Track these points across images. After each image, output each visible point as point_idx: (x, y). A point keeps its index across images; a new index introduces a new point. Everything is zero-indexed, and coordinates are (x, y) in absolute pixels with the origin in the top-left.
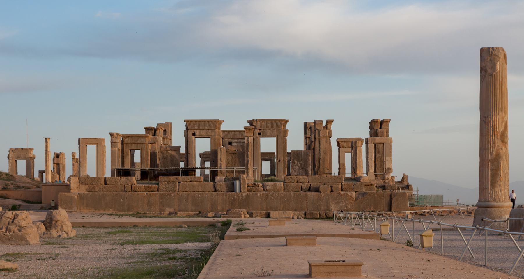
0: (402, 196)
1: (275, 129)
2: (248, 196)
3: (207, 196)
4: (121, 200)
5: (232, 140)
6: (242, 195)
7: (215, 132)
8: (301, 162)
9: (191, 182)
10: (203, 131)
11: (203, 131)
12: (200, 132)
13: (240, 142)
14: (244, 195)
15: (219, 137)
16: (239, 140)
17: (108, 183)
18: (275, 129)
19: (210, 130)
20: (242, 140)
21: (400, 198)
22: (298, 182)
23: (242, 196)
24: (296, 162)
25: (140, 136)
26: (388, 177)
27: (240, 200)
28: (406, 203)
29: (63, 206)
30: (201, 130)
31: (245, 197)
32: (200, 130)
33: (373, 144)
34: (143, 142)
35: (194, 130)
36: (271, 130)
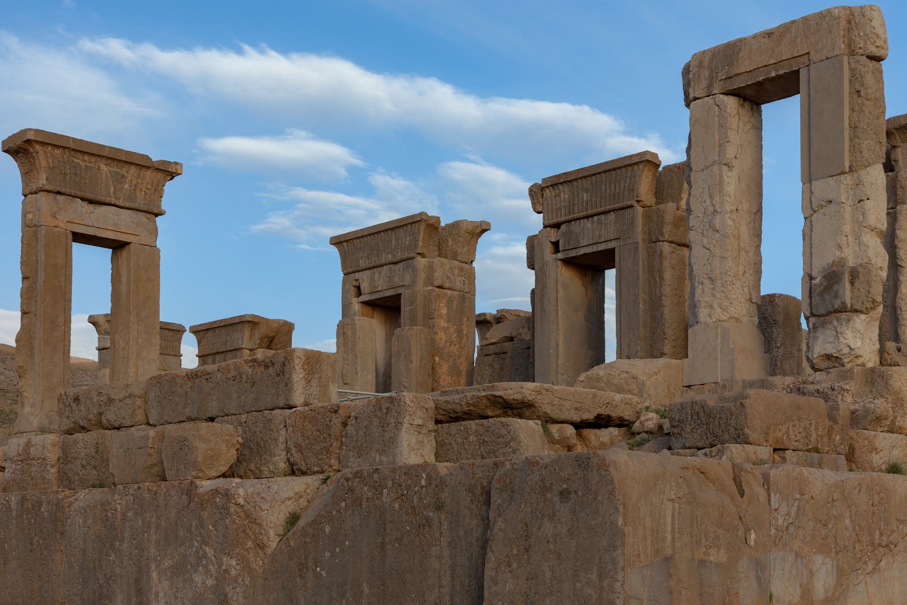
0: (564, 495)
1: (609, 212)
7: (414, 270)
10: (380, 273)
11: (380, 273)
12: (372, 280)
15: (430, 288)
18: (609, 212)
19: (400, 265)
21: (552, 517)
25: (229, 325)
26: (830, 350)
28: (601, 577)
30: (375, 270)
32: (371, 271)
33: (728, 93)
34: (236, 347)
35: (357, 275)
36: (595, 218)
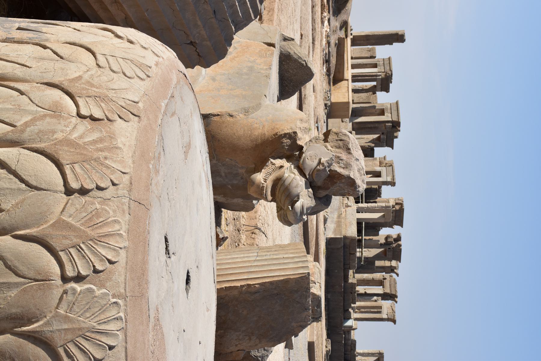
2: (341, 334)
3: (341, 314)
4: (336, 271)
5: (386, 135)
6: (342, 331)
8: (366, 266)
9: (351, 299)
13: (384, 140)
14: (342, 332)
16: (385, 139)
17: (352, 256)
20: (385, 141)
22: (351, 349)
23: (340, 331)
24: (366, 263)
27: (337, 330)
29: (331, 240)
31: (340, 332)
35: (394, 213)
